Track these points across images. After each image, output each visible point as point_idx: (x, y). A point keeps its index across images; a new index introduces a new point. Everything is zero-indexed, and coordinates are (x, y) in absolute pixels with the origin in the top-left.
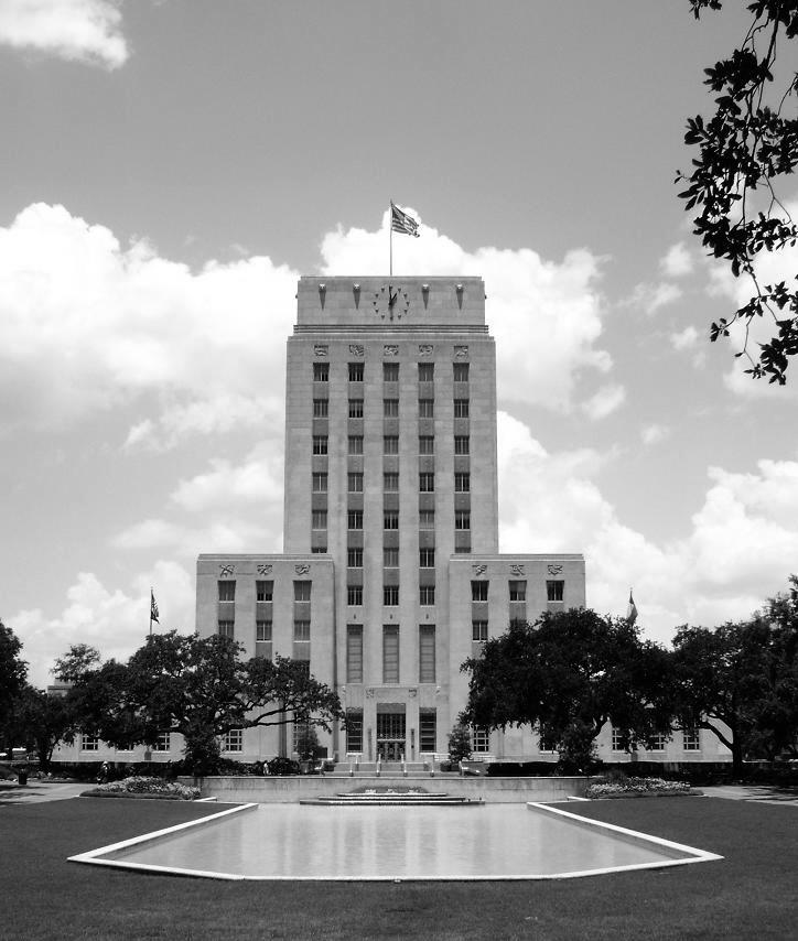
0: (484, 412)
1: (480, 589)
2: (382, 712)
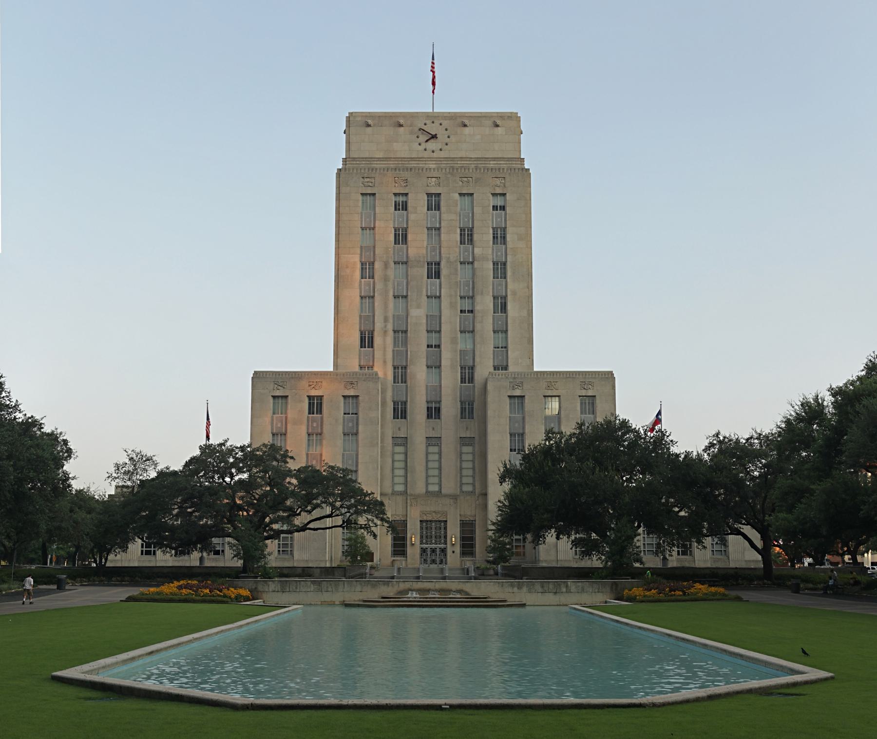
2: (425, 518)
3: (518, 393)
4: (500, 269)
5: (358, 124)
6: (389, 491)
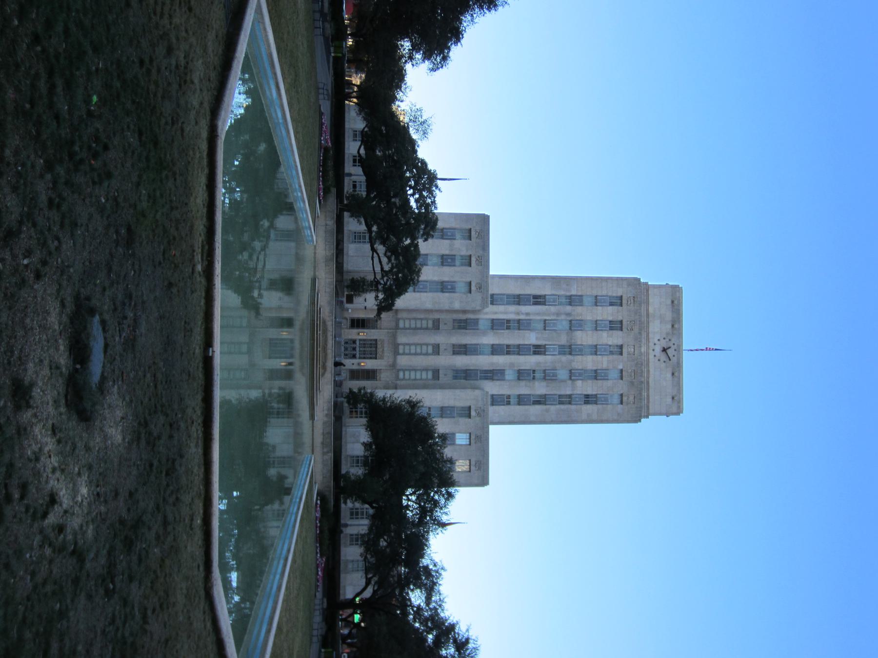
0: (589, 415)
1: (467, 412)
2: (379, 343)
3: (473, 413)
4: (567, 400)
5: (674, 294)
6: (400, 316)
